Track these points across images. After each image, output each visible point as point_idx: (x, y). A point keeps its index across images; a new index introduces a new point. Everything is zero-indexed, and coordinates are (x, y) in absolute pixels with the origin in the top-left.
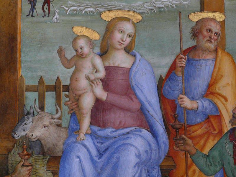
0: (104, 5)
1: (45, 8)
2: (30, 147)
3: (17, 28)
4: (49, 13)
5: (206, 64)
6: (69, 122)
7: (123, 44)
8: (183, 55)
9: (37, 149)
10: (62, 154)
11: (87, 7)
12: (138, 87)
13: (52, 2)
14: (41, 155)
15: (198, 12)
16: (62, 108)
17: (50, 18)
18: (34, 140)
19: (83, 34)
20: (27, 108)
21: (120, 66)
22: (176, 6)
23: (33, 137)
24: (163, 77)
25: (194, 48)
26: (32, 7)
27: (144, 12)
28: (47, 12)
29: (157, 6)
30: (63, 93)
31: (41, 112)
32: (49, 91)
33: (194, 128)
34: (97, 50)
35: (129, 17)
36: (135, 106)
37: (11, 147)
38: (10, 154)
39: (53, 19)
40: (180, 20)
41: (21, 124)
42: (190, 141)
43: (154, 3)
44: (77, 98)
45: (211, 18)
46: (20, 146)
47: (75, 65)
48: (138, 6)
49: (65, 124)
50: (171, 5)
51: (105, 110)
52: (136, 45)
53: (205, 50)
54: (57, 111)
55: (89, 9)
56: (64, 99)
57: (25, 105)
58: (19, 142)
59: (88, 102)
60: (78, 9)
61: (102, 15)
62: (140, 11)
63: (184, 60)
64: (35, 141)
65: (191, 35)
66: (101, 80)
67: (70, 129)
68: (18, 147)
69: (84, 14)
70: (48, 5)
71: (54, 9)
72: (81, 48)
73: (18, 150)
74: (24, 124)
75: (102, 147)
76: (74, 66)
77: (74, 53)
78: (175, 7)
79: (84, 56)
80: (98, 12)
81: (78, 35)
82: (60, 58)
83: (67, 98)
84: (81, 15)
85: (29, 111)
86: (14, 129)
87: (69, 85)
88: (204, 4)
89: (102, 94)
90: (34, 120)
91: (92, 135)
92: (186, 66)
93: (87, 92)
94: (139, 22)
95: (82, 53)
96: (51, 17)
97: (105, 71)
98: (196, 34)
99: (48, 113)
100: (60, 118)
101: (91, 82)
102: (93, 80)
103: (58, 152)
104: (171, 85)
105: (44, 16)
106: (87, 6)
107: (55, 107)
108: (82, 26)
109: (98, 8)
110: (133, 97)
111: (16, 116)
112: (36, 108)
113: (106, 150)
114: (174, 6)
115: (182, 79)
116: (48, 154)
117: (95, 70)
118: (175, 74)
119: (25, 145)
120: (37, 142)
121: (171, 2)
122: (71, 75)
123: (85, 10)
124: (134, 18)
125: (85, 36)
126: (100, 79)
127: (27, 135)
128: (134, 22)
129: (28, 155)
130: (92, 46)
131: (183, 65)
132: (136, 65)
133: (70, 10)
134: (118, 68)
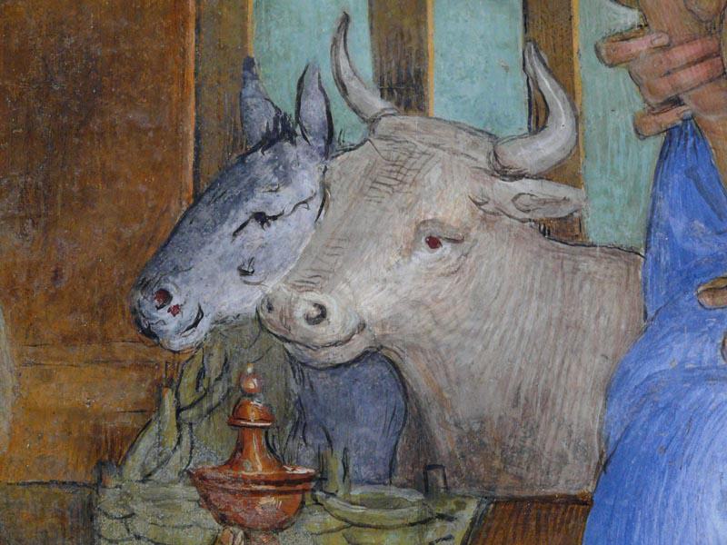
6: (644, 203)
10: (597, 478)
14: (403, 486)
16: (578, 88)
18: (341, 355)
23: (324, 332)
31: (398, 120)
37: (128, 421)
38: (112, 482)
41: (223, 216)
46: (210, 411)
54: (539, 115)
57: (249, 63)
58: (201, 374)
64: (347, 365)
67: (657, 262)
68: (189, 415)
73: (186, 440)
74: (243, 217)
83: (623, 10)
85: (289, 109)
90: (335, 187)
99: (458, 126)
100: (564, 172)
103: (563, 458)
107: (523, 81)
111: (176, 145)
112: (352, 85)
116: (471, 482)
119: (251, 395)
120: (371, 370)
127: (270, 309)
129: (285, 485)
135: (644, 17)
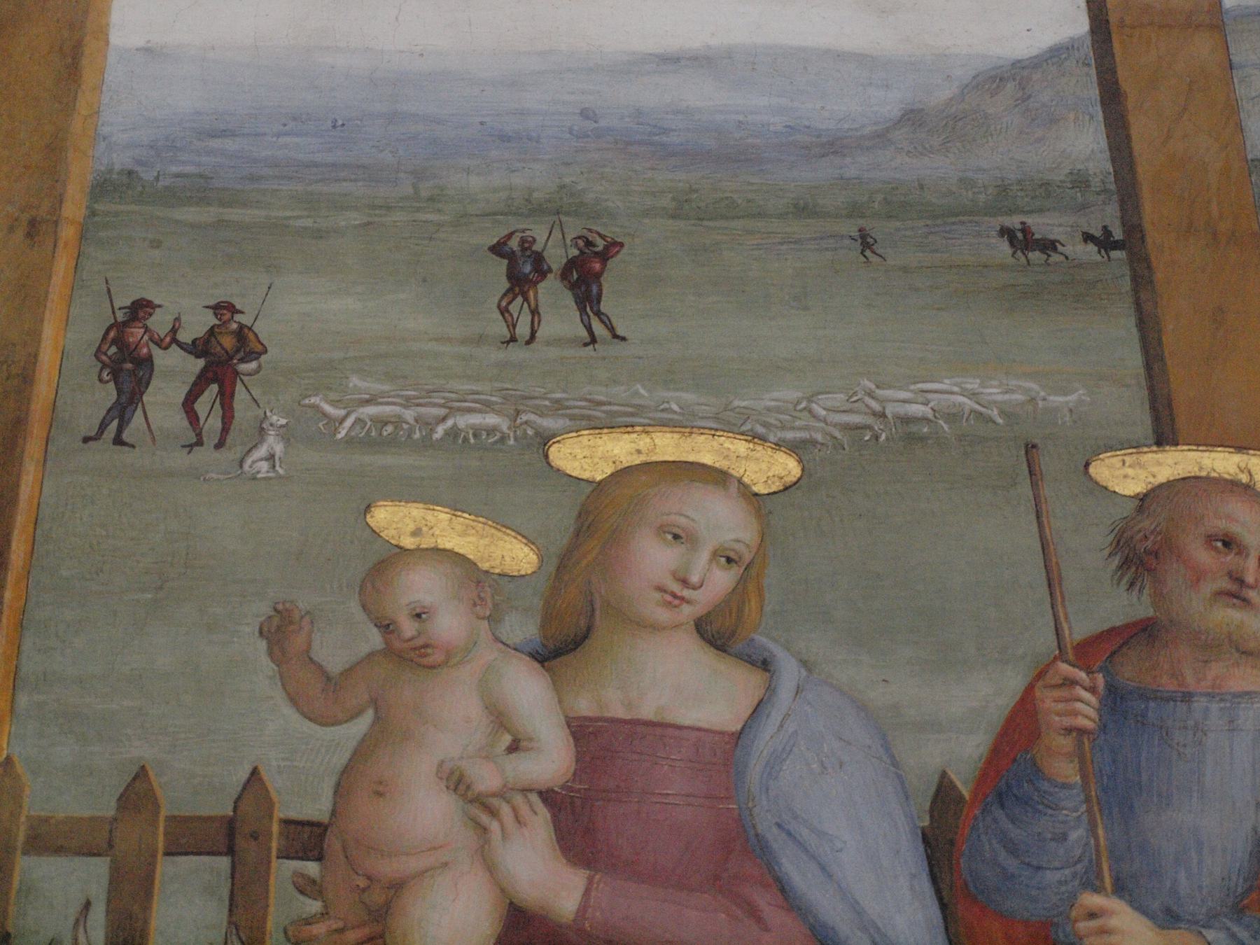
0: (568, 399)
1: (202, 406)
3: (14, 501)
4: (225, 430)
5: (1231, 722)
7: (688, 602)
8: (1073, 666)
11: (459, 409)
12: (801, 845)
13: (245, 378)
15: (1145, 449)
17: (228, 455)
19: (432, 546)
21: (670, 718)
22: (1002, 413)
24: (959, 784)
26: (124, 399)
27: (814, 443)
28: (212, 424)
29: (890, 416)
30: (284, 870)
32: (186, 854)
35: (721, 464)
39: (249, 461)
40: (1034, 485)
43: (873, 398)
44: (377, 897)
45: (1226, 476)
47: (375, 702)
48: (778, 410)
50: (972, 411)
52: (767, 609)
55: (475, 419)
60: (409, 415)
61: (552, 449)
62: (790, 435)
63: (1086, 695)
65: (1116, 561)
66: (547, 796)
69: (437, 440)
70: (221, 393)
71: (261, 412)
72: (418, 616)
76: (369, 716)
77: (375, 639)
78: (1000, 421)
79: (437, 657)
80: (530, 432)
81: (401, 548)
82: (278, 666)
83: (309, 901)
84: (427, 444)
87: (325, 818)
88: (1170, 406)
92: (1103, 728)
93: (446, 864)
94: (786, 489)
95: (419, 642)
96: (239, 448)
97: (573, 746)
102: (494, 795)
104: (1015, 832)
105: (191, 446)
106: (465, 401)
108: (430, 500)
109: (532, 417)
110: (764, 901)
114: (994, 413)
115: (1088, 800)
117: (507, 739)
118: (1037, 771)
121: (973, 395)
122: (340, 759)
123: (450, 423)
124: (752, 466)
125: (444, 550)
126: (540, 793)
128: (756, 489)
130: (489, 601)
131: (1082, 722)
132: (776, 716)
133: (358, 420)
134: (659, 731)
135: (326, 907)
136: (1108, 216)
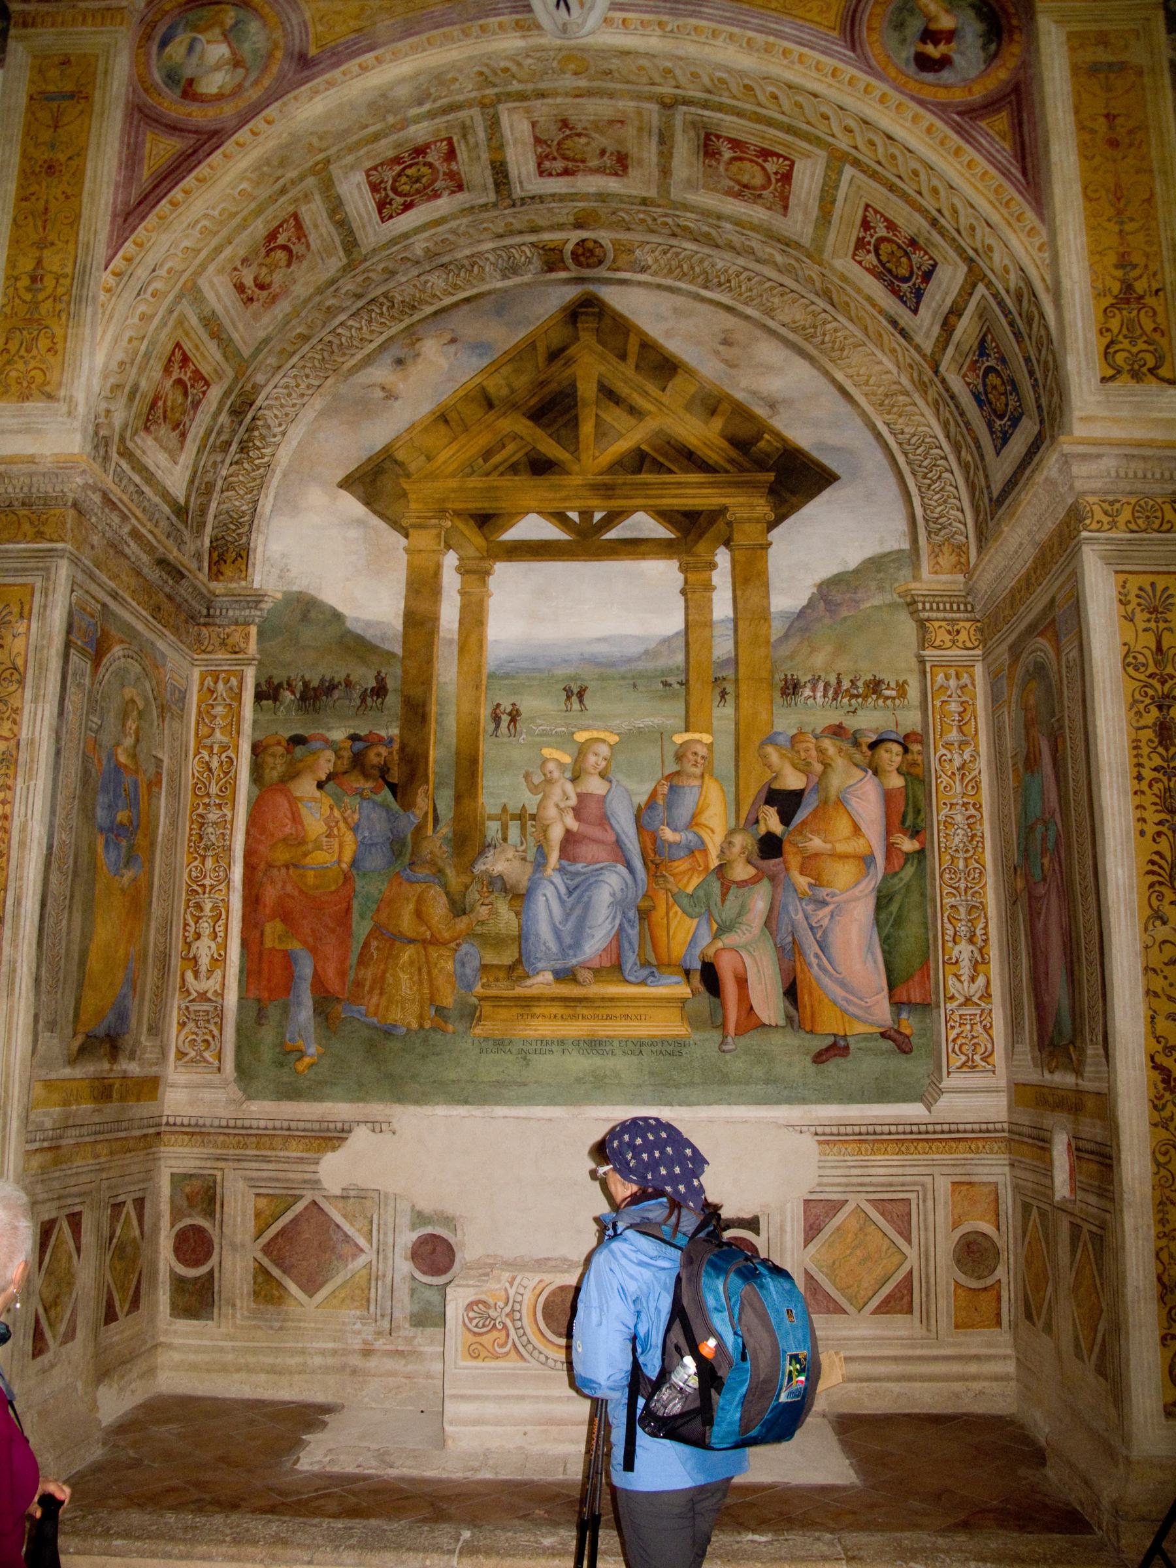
2: (491, 884)
9: (499, 885)
20: (489, 839)
25: (677, 773)
33: (676, 864)
34: (568, 775)
36: (610, 838)
42: (671, 879)
49: (530, 856)
51: (575, 842)
53: (689, 776)
56: (530, 830)
59: (556, 834)
75: (572, 884)
86: (473, 863)
89: (573, 825)
91: (561, 870)
98: (679, 758)
101: (561, 810)
113: (576, 888)
136: (682, 678)
